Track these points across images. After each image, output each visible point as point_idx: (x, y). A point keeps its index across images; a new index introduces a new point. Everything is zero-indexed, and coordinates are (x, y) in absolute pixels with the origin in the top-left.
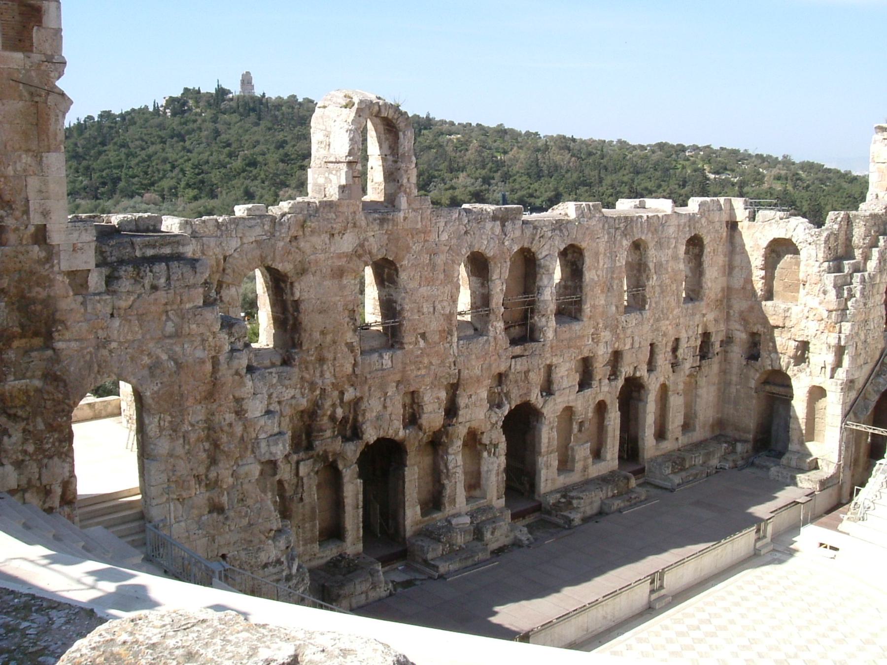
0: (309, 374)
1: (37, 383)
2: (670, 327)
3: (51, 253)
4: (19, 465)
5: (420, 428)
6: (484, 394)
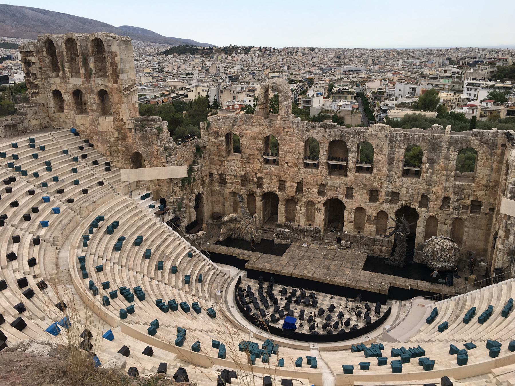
2: (439, 191)
3: (125, 124)
4: (121, 163)
6: (316, 191)
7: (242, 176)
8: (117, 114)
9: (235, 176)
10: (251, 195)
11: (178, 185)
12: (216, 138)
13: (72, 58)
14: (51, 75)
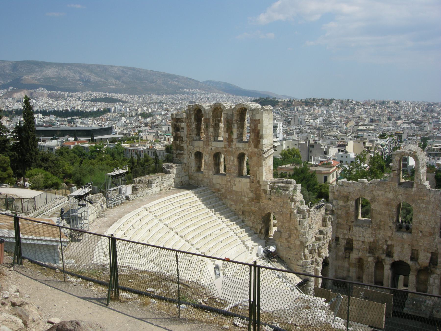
0: (375, 231)
1: (257, 209)
3: (260, 186)
5: (418, 263)
7: (371, 242)
8: (253, 175)
9: (363, 242)
10: (379, 264)
11: (309, 248)
12: (344, 202)
13: (216, 124)
14: (195, 138)
